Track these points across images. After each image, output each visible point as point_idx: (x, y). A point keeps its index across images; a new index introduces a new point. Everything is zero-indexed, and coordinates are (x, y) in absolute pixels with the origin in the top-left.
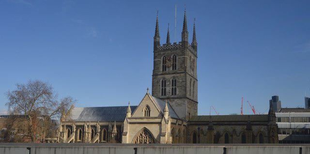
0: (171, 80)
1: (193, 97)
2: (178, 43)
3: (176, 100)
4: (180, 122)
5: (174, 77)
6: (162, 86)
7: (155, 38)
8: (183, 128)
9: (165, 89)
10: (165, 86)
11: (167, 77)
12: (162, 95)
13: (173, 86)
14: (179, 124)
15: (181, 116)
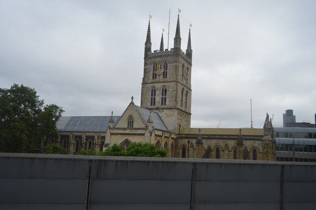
0: (161, 89)
1: (186, 108)
2: (169, 50)
3: (165, 111)
4: (167, 135)
5: (164, 86)
6: (152, 95)
7: (146, 44)
8: (170, 141)
9: (155, 98)
10: (155, 95)
11: (158, 86)
12: (151, 105)
13: (163, 95)
14: (165, 137)
15: (170, 128)
